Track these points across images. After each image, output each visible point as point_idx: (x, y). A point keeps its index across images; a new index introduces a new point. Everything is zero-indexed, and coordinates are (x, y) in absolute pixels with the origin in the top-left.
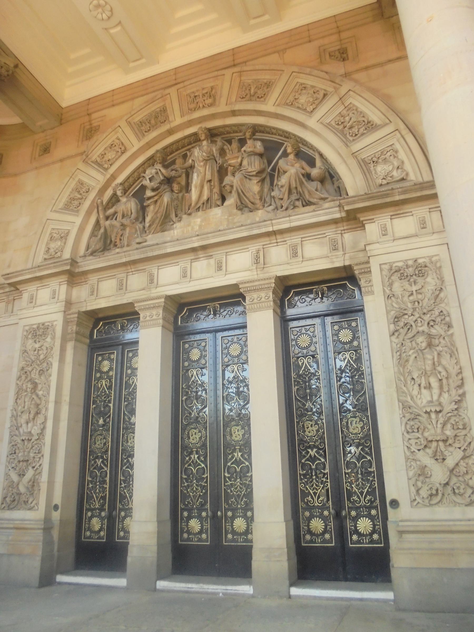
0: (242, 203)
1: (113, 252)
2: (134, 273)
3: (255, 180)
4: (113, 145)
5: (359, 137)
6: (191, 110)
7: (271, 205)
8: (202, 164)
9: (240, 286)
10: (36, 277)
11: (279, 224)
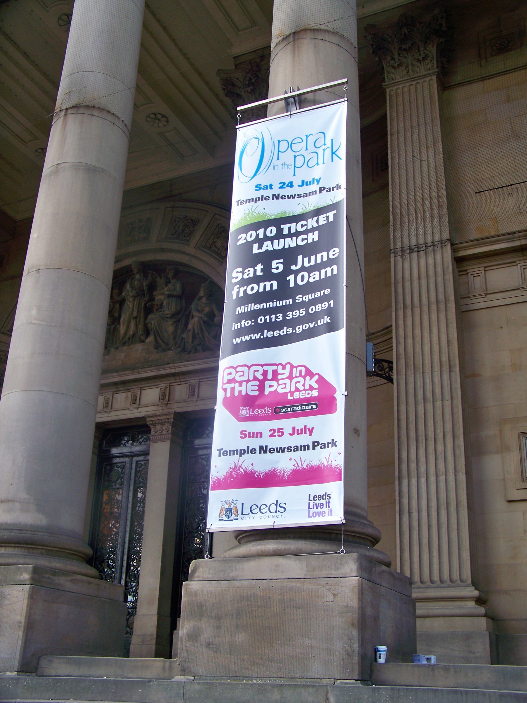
9: (148, 419)
11: (179, 367)
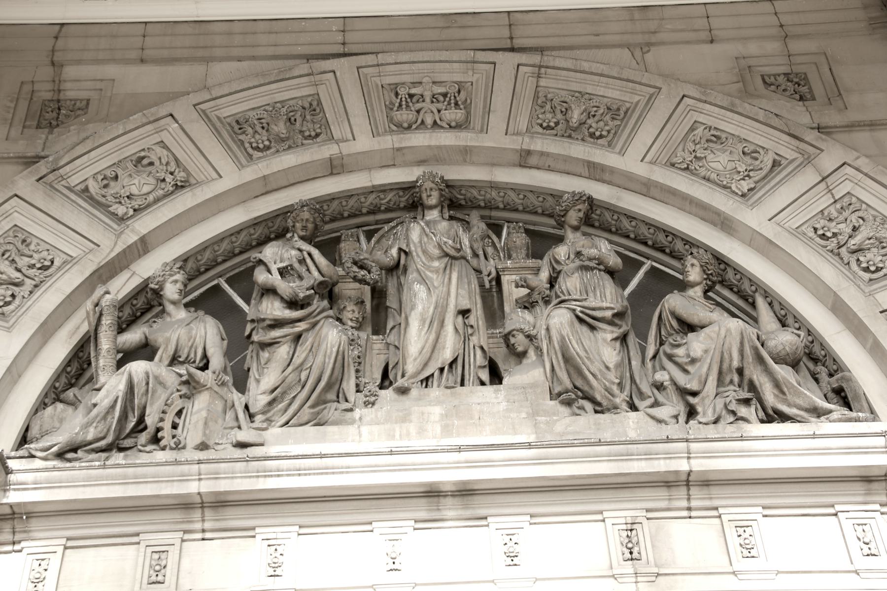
0: (576, 387)
1: (144, 458)
2: (208, 535)
3: (608, 334)
4: (145, 162)
6: (399, 125)
7: (656, 404)
8: (436, 264)
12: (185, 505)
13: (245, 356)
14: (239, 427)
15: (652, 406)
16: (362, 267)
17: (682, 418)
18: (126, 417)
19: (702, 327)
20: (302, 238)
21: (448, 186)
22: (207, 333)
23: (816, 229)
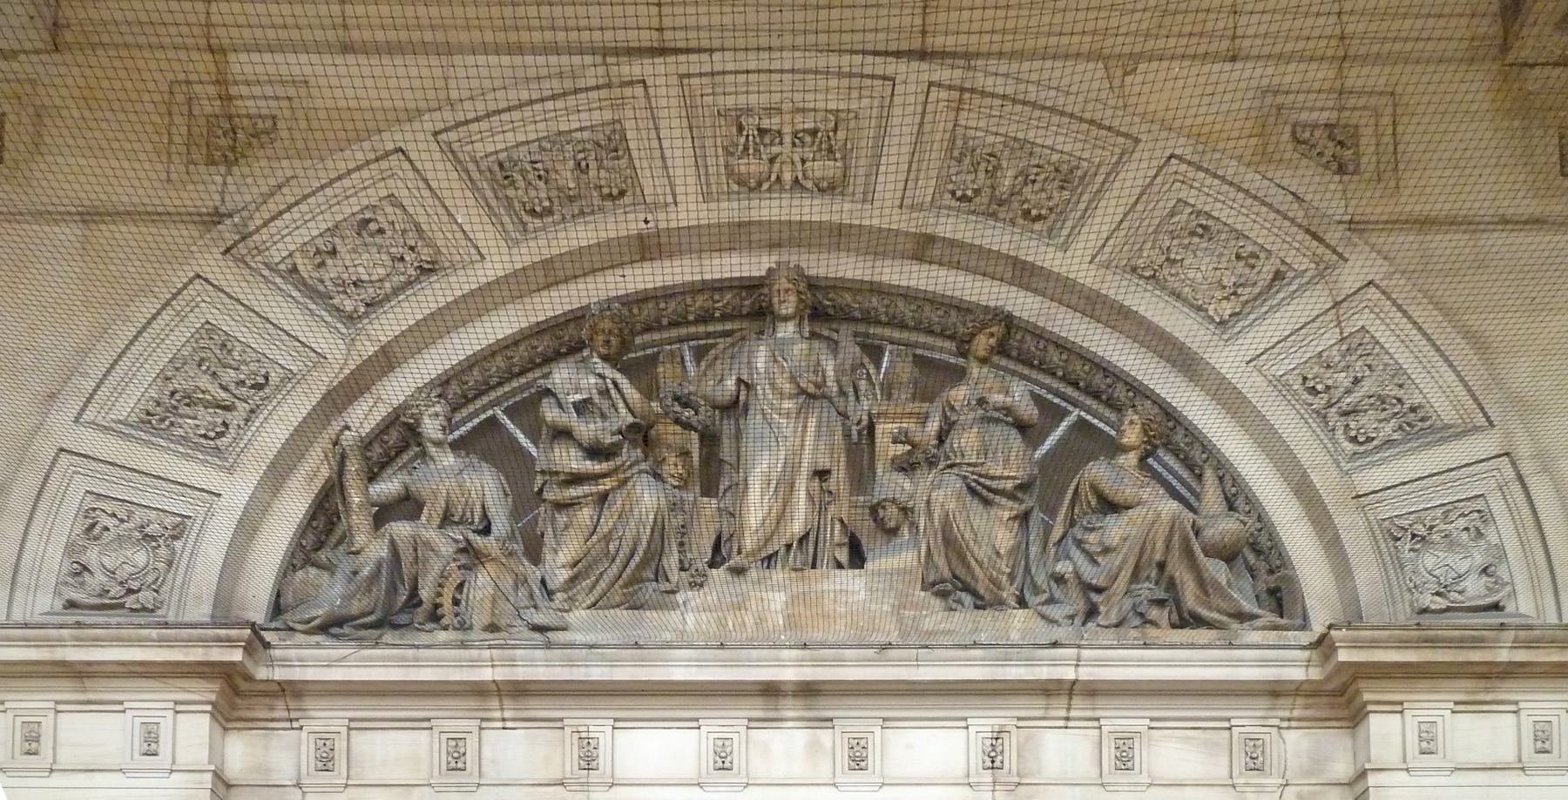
0: (955, 576)
2: (509, 724)
3: (1006, 510)
4: (373, 226)
5: (1378, 448)
7: (1051, 601)
8: (788, 404)
10: (63, 663)
12: (478, 691)
13: (535, 519)
14: (535, 607)
15: (1043, 604)
16: (686, 405)
17: (1078, 621)
18: (396, 590)
19: (1128, 508)
20: (605, 358)
21: (811, 286)
22: (484, 486)
23: (1305, 379)
